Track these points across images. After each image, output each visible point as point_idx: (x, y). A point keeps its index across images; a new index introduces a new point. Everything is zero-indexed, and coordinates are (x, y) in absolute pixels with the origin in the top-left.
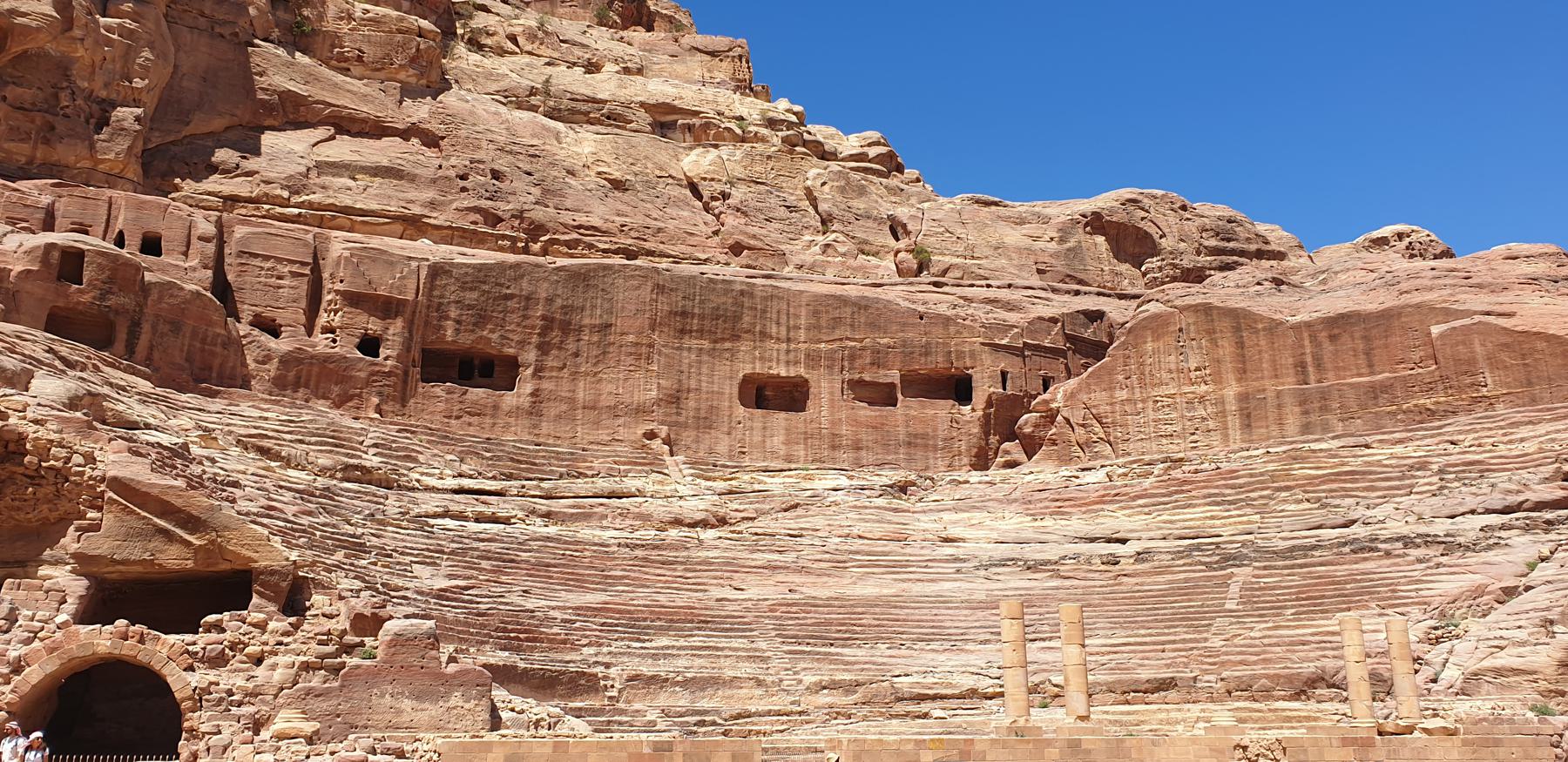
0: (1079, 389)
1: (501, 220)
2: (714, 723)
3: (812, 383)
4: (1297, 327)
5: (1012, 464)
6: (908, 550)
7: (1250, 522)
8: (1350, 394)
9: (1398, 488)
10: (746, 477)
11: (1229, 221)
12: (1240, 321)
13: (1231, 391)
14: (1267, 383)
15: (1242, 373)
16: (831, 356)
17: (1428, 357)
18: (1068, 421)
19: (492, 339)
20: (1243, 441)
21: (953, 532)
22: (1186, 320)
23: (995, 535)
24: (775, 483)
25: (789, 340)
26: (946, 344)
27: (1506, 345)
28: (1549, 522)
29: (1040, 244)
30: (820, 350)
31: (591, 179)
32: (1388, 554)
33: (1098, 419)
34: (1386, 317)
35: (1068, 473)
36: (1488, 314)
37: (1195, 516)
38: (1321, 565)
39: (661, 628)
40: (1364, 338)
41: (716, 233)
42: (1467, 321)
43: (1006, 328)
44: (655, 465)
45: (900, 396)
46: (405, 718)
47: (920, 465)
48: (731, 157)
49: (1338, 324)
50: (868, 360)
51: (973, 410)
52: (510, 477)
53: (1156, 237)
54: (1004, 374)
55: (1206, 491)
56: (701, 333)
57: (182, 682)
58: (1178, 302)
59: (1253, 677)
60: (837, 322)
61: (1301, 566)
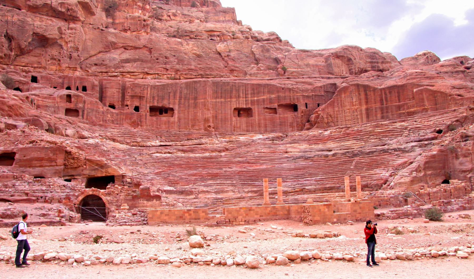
0: (325, 108)
1: (167, 70)
2: (221, 201)
3: (253, 110)
4: (381, 90)
5: (308, 129)
6: (276, 156)
7: (362, 145)
8: (394, 108)
9: (399, 135)
10: (234, 137)
11: (374, 53)
12: (366, 88)
13: (364, 107)
14: (373, 105)
15: (367, 103)
16: (258, 101)
19: (166, 103)
21: (289, 150)
22: (352, 88)
23: (298, 150)
24: (242, 138)
25: (246, 97)
26: (290, 96)
27: (432, 95)
28: (426, 144)
29: (320, 63)
30: (254, 100)
31: (191, 55)
34: (403, 86)
35: (321, 132)
38: (375, 156)
39: (210, 179)
40: (397, 92)
41: (226, 67)
42: (422, 88)
43: (307, 90)
44: (209, 135)
46: (145, 205)
47: (284, 130)
48: (231, 44)
50: (268, 102)
52: (172, 141)
53: (353, 59)
54: (306, 104)
56: (221, 97)
57: (104, 198)
58: (350, 83)
60: (258, 93)
61: (371, 157)
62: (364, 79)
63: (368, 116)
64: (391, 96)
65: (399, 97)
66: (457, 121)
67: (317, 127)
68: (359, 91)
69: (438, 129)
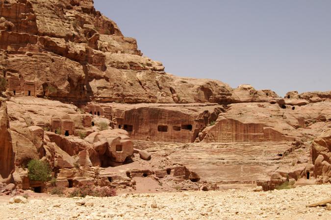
5: (198, 142)
12: (237, 122)
13: (234, 134)
14: (240, 133)
15: (236, 131)
21: (199, 157)
22: (229, 121)
32: (260, 165)
33: (213, 135)
37: (233, 156)
49: (251, 125)
60: (172, 115)
67: (204, 141)
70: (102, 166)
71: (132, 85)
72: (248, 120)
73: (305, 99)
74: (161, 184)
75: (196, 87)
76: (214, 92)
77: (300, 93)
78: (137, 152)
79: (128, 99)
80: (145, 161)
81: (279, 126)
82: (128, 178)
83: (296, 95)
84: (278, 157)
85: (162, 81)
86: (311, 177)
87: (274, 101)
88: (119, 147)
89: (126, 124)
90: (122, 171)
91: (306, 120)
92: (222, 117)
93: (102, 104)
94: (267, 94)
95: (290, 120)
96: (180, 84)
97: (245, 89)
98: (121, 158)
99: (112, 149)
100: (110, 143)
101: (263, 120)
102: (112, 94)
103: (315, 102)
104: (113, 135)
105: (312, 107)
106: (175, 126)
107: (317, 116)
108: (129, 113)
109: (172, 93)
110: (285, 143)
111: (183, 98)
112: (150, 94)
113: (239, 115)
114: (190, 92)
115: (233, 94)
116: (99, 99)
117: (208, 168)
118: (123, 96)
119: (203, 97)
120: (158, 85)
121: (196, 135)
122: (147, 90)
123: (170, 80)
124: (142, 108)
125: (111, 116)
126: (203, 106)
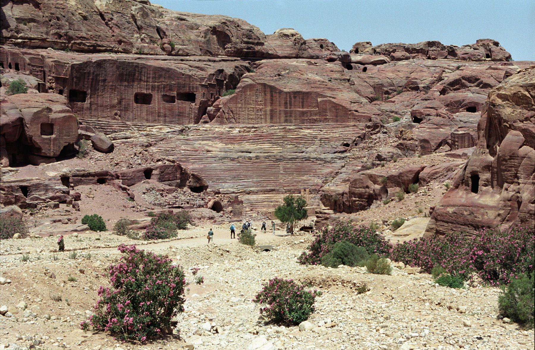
4: (286, 93)
5: (206, 122)
8: (298, 113)
12: (273, 89)
13: (269, 108)
14: (278, 107)
15: (272, 104)
17: (316, 106)
18: (223, 111)
20: (271, 122)
21: (207, 148)
22: (259, 87)
23: (218, 150)
24: (154, 131)
26: (190, 84)
27: (334, 107)
30: (155, 85)
32: (313, 162)
33: (232, 111)
34: (308, 94)
36: (330, 97)
37: (266, 146)
45: (176, 100)
49: (296, 94)
51: (196, 105)
54: (204, 93)
55: (267, 139)
56: (125, 81)
58: (257, 81)
59: (291, 189)
60: (160, 76)
62: (269, 78)
63: (272, 118)
64: (295, 101)
65: (303, 102)
66: (359, 137)
67: (217, 121)
68: (265, 91)
69: (345, 142)
70: (13, 164)
71: (85, 18)
72: (290, 86)
73: (384, 54)
74: (132, 199)
75: (203, 29)
76: (233, 39)
77: (374, 45)
78: (88, 138)
79: (79, 44)
80: (100, 154)
81: (344, 96)
82: (64, 188)
83: (369, 49)
84: (342, 148)
85: (142, 16)
86: (484, 188)
87: (333, 56)
88: (48, 128)
89: (74, 88)
90: (52, 174)
91: (385, 89)
92: (247, 80)
93: (24, 50)
94: (322, 47)
95: (360, 88)
96: (175, 23)
97: (286, 36)
98: (53, 150)
99: (33, 131)
100: (27, 119)
101: (319, 86)
102: (47, 33)
103: (399, 59)
104: (33, 104)
105: (395, 67)
106: (166, 95)
107: (404, 82)
108: (79, 70)
109: (162, 38)
110: (355, 125)
111: (180, 47)
112: (121, 38)
113: (277, 77)
114: (193, 37)
115: (265, 43)
116: (20, 40)
117: (223, 167)
118: (70, 38)
119: (215, 46)
120: (136, 22)
121: (203, 110)
122: (115, 30)
123: (157, 15)
124: (105, 60)
125: (44, 73)
126: (214, 61)
